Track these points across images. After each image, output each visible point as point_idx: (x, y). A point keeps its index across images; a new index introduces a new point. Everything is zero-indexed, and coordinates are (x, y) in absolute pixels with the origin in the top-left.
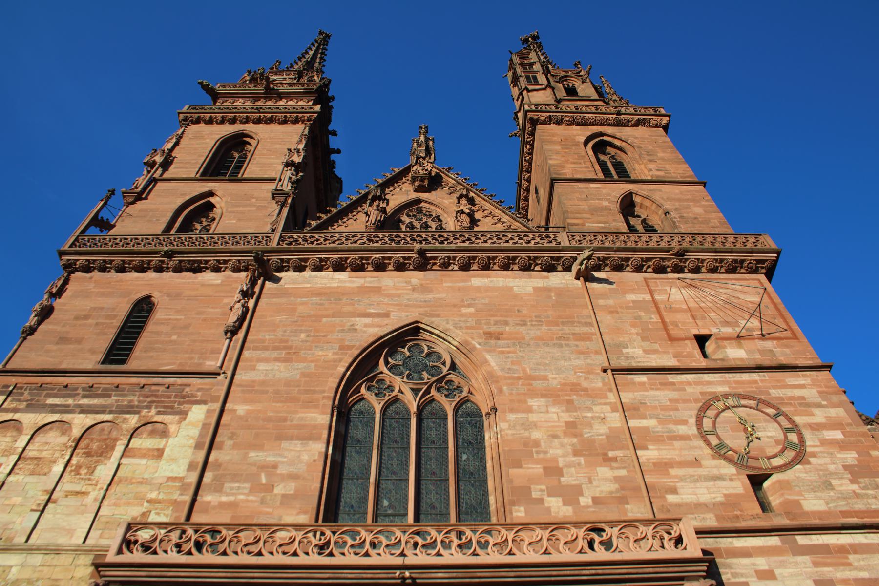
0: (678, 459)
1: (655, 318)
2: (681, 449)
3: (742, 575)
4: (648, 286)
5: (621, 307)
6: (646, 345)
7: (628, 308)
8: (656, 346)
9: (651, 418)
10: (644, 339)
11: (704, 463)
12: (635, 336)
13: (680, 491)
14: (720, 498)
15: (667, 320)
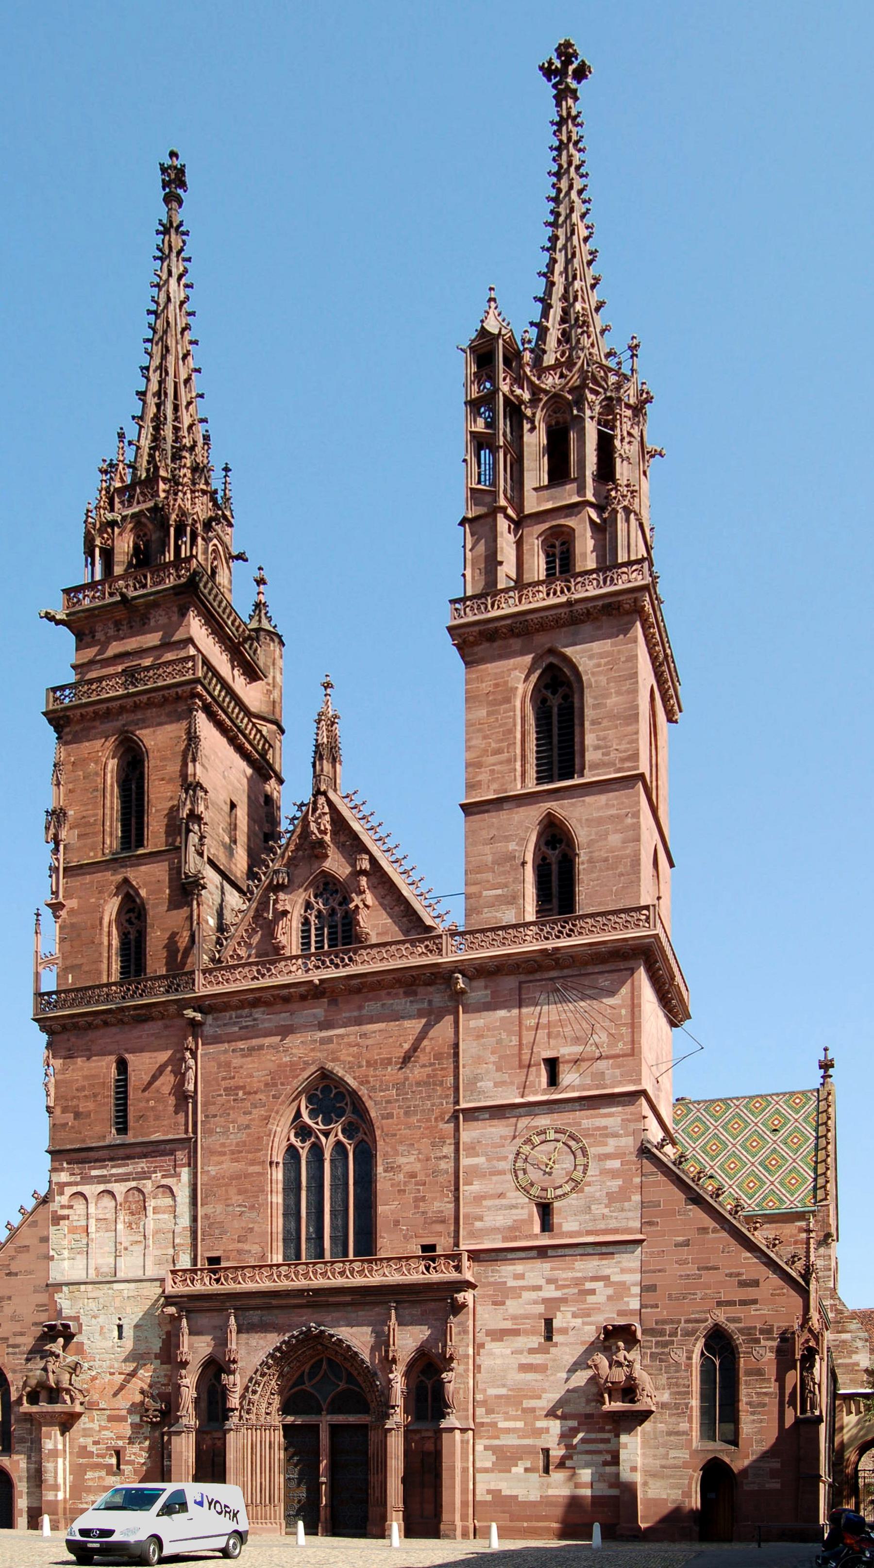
0: (491, 1192)
1: (515, 1041)
2: (496, 1183)
3: (505, 1277)
4: (520, 995)
5: (488, 1030)
6: (498, 1076)
7: (495, 1029)
8: (506, 1077)
9: (483, 1155)
10: (499, 1069)
11: (508, 1194)
12: (491, 1066)
13: (485, 1218)
14: (509, 1223)
15: (524, 1042)
